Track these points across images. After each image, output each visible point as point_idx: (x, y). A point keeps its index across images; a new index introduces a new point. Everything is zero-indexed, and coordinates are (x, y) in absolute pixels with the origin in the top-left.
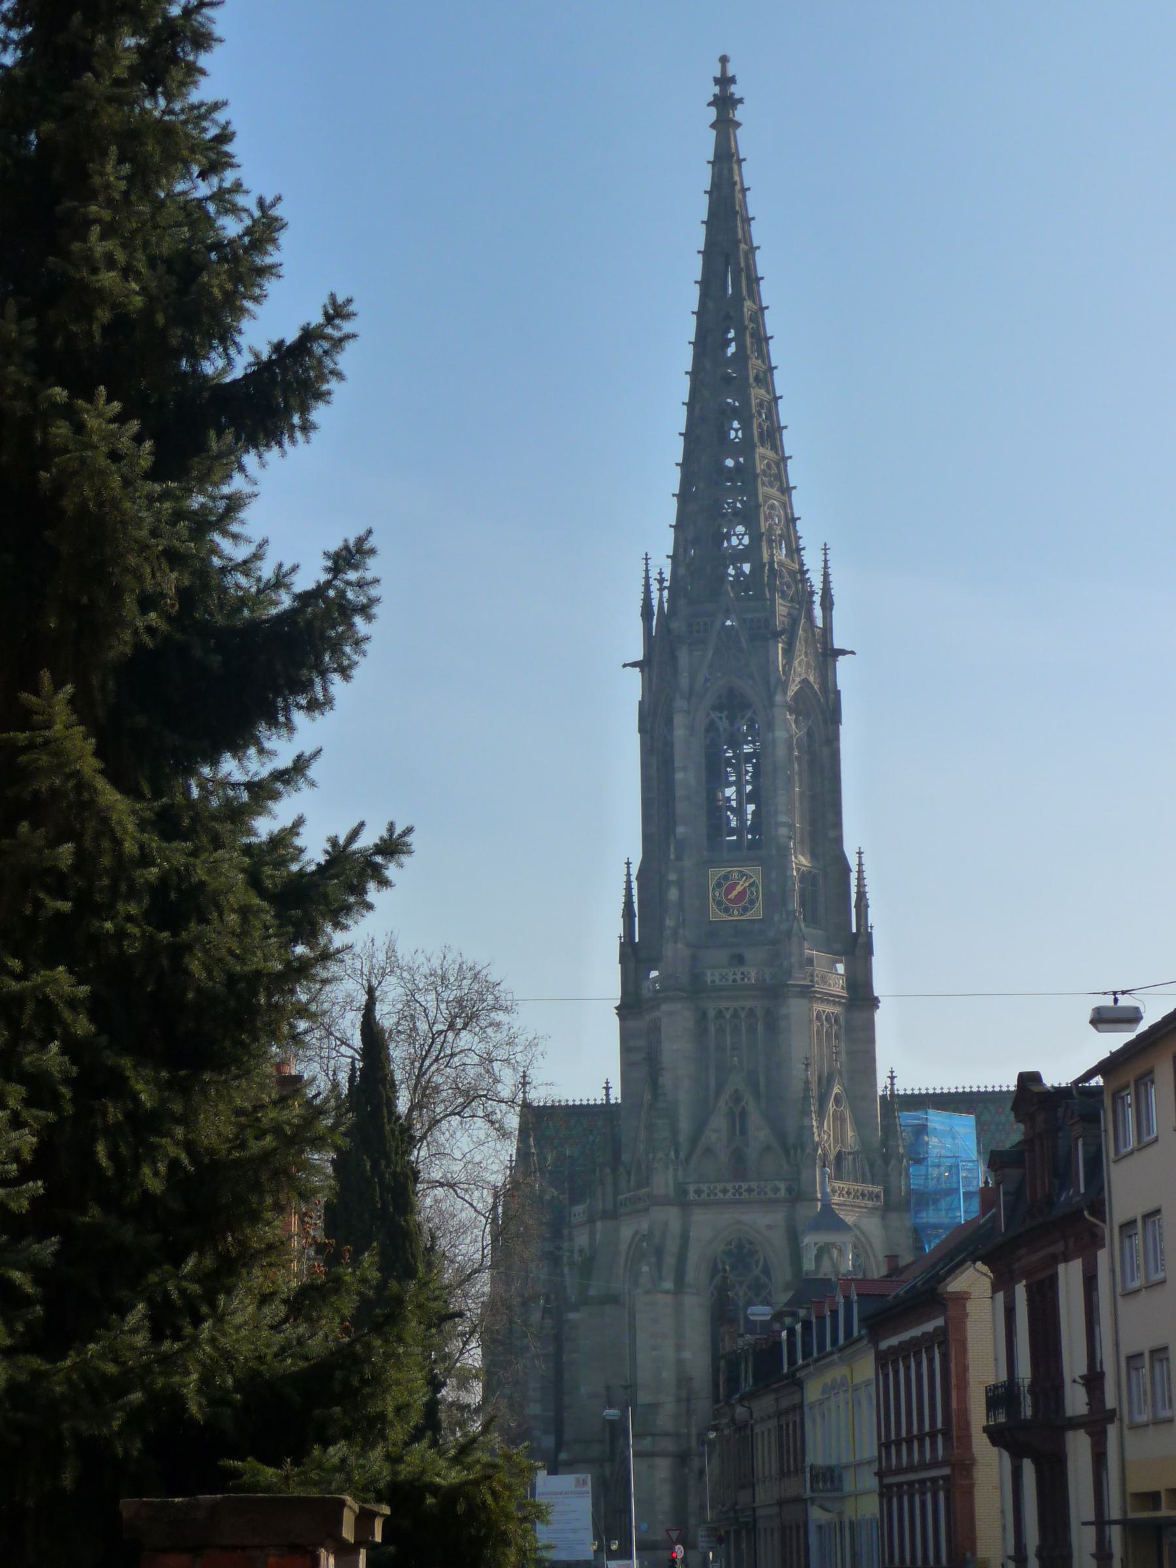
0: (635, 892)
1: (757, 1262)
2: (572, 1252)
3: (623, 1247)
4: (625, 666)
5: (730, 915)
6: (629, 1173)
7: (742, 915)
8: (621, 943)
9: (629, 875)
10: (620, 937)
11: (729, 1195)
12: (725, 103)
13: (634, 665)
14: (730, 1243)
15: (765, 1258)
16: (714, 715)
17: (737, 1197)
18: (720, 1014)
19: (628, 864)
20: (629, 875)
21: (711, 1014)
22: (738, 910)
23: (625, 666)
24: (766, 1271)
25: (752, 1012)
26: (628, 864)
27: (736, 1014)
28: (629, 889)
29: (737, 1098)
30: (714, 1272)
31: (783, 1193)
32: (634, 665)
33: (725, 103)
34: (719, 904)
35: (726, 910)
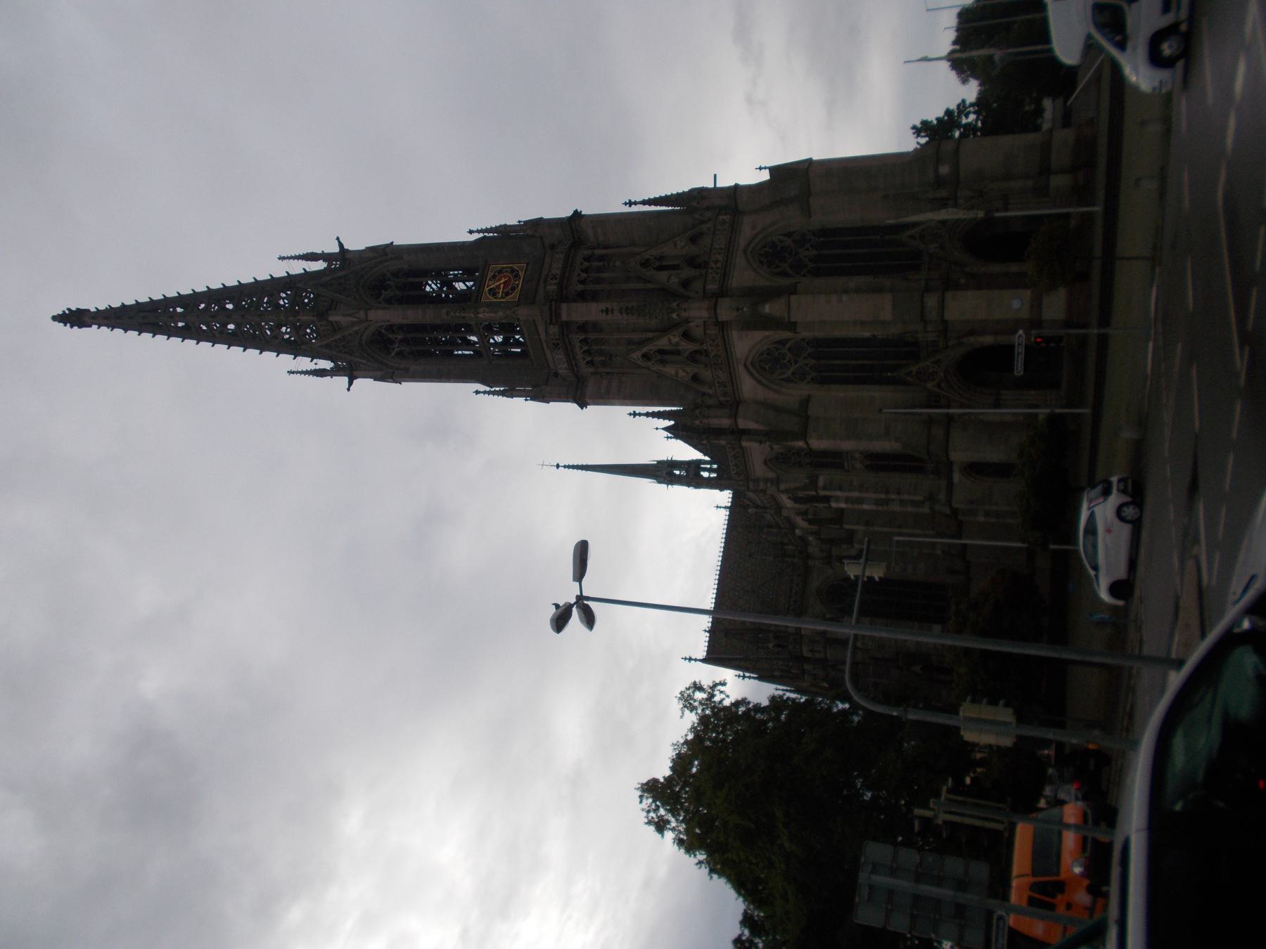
0: (497, 389)
1: (781, 242)
2: (767, 480)
3: (762, 393)
4: (349, 390)
5: (518, 286)
6: (704, 394)
7: (520, 278)
8: (531, 400)
9: (485, 392)
10: (526, 400)
11: (720, 258)
12: (76, 318)
13: (350, 383)
14: (762, 263)
15: (784, 235)
16: (381, 299)
17: (723, 251)
18: (582, 282)
19: (477, 392)
20: (485, 392)
21: (580, 287)
22: (515, 281)
23: (349, 390)
24: (789, 235)
25: (588, 259)
26: (477, 392)
27: (586, 271)
28: (494, 393)
29: (645, 264)
30: (784, 274)
31: (727, 218)
32: (350, 383)
33: (76, 318)
34: (507, 294)
35: (513, 289)
